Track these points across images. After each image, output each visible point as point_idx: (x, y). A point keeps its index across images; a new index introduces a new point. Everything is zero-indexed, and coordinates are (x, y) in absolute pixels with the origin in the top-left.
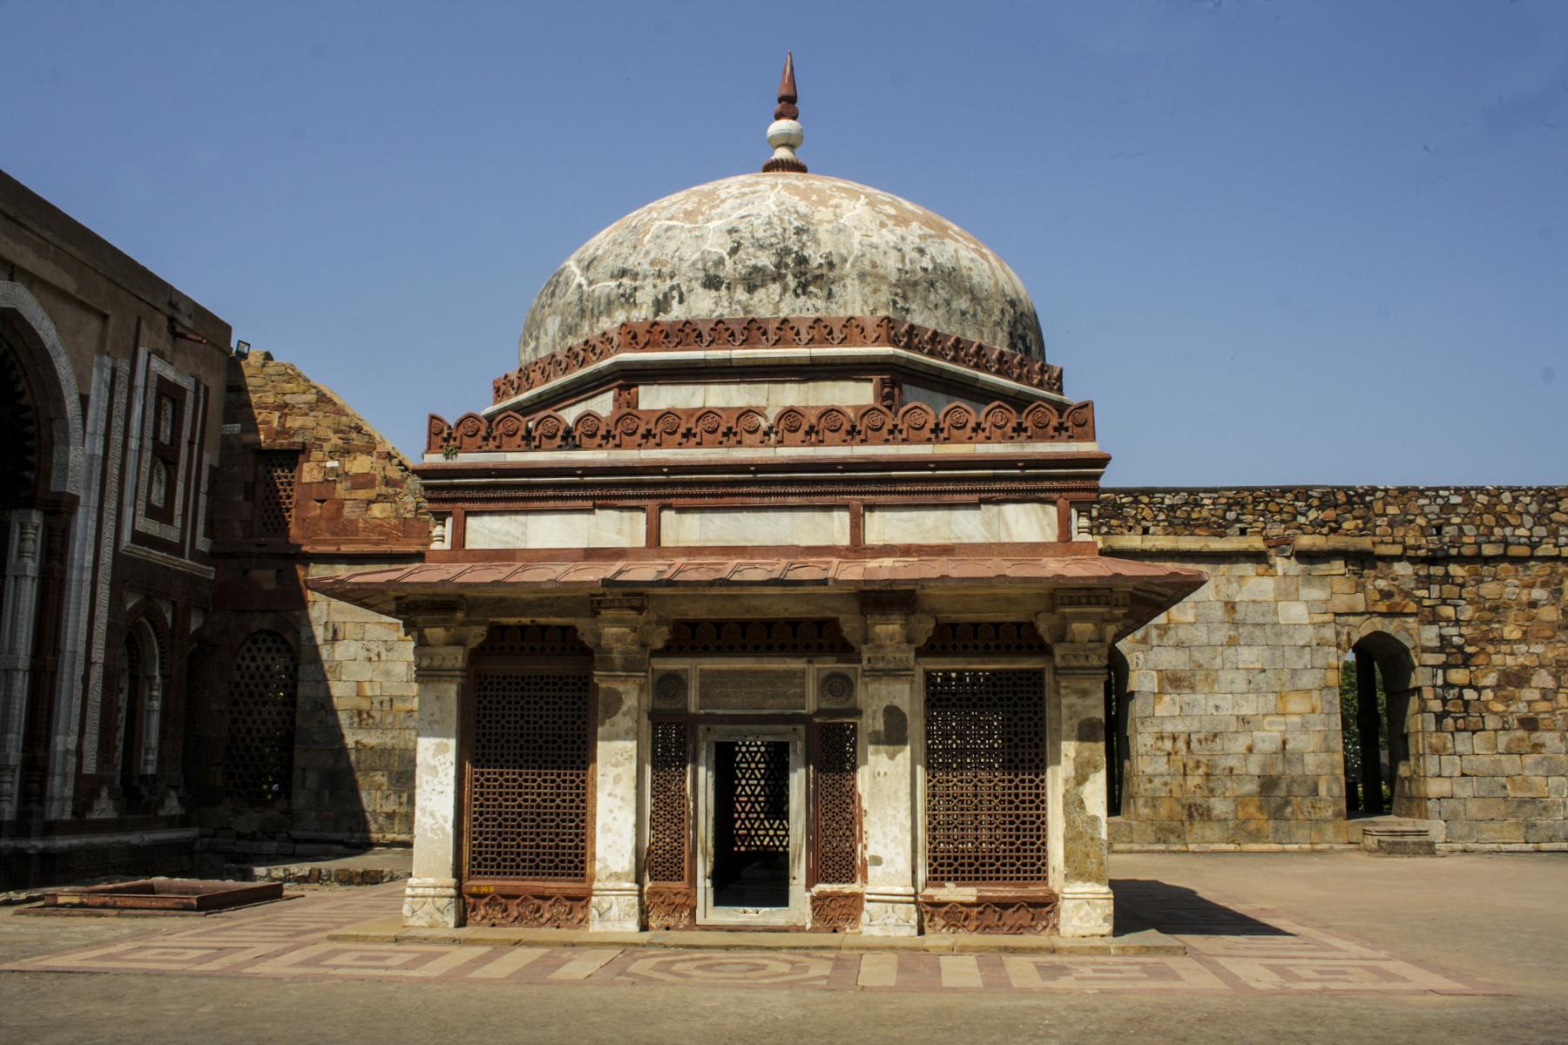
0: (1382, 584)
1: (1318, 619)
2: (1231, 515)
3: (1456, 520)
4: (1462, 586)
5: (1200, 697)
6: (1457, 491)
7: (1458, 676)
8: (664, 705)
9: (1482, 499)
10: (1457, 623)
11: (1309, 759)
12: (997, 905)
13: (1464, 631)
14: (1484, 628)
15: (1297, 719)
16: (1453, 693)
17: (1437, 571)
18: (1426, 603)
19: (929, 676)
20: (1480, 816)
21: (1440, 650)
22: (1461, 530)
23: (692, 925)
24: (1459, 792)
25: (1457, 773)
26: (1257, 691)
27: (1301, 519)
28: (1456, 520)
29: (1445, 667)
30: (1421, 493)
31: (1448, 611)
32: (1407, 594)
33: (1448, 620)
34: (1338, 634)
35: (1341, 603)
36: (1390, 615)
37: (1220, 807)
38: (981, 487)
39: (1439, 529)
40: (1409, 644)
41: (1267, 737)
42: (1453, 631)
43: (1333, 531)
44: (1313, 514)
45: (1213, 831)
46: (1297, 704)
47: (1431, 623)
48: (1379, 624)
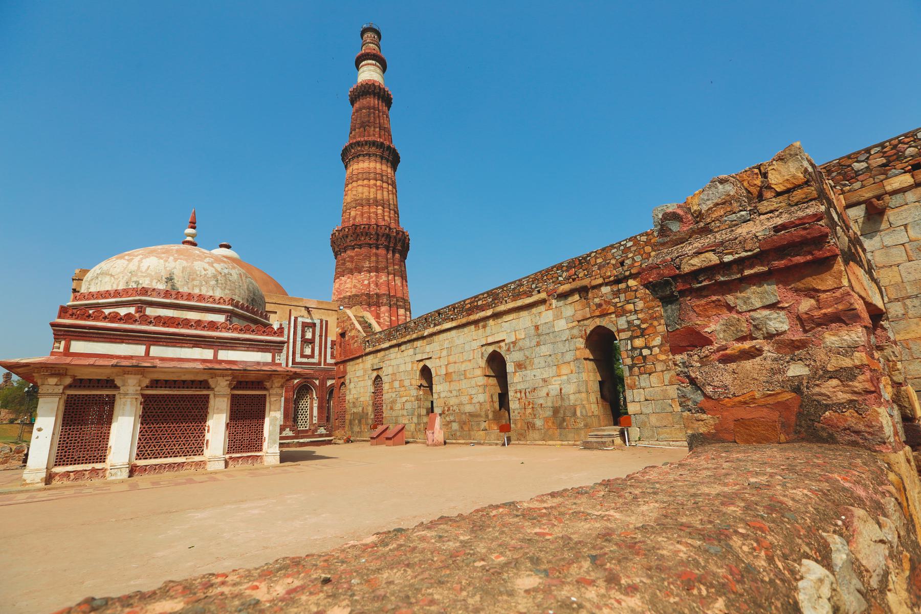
0: (597, 300)
1: (571, 325)
2: (534, 286)
3: (630, 255)
4: (636, 291)
5: (528, 372)
6: (630, 240)
7: (638, 342)
9: (644, 238)
10: (636, 312)
11: (572, 397)
13: (640, 316)
14: (651, 312)
15: (565, 377)
16: (637, 352)
17: (622, 286)
18: (619, 305)
20: (657, 424)
21: (628, 329)
22: (633, 259)
24: (645, 411)
25: (643, 399)
26: (549, 366)
27: (560, 279)
28: (630, 255)
29: (632, 338)
30: (612, 247)
31: (630, 307)
32: (608, 303)
33: (630, 312)
34: (581, 331)
35: (579, 316)
36: (603, 315)
37: (539, 423)
39: (622, 264)
40: (614, 329)
41: (554, 388)
42: (633, 317)
43: (574, 280)
44: (565, 274)
45: (536, 435)
46: (565, 370)
47: (622, 316)
48: (598, 322)
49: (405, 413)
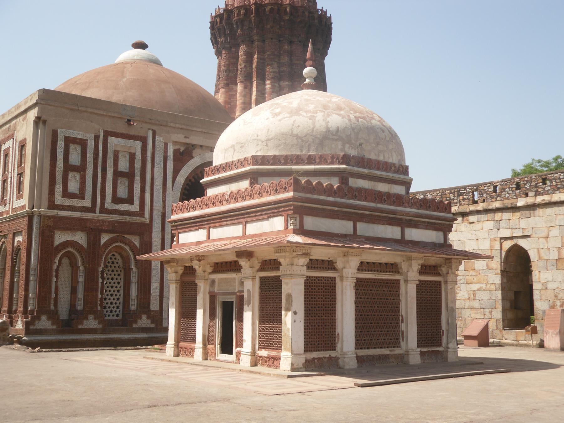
8: (211, 290)
12: (272, 358)
19: (262, 279)
23: (215, 360)
38: (267, 212)
49: (476, 304)
